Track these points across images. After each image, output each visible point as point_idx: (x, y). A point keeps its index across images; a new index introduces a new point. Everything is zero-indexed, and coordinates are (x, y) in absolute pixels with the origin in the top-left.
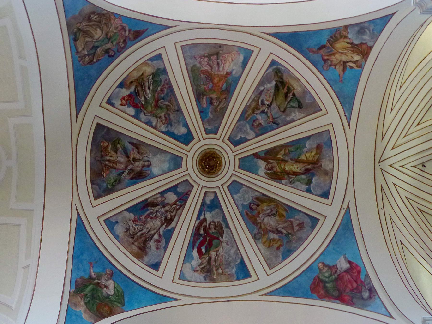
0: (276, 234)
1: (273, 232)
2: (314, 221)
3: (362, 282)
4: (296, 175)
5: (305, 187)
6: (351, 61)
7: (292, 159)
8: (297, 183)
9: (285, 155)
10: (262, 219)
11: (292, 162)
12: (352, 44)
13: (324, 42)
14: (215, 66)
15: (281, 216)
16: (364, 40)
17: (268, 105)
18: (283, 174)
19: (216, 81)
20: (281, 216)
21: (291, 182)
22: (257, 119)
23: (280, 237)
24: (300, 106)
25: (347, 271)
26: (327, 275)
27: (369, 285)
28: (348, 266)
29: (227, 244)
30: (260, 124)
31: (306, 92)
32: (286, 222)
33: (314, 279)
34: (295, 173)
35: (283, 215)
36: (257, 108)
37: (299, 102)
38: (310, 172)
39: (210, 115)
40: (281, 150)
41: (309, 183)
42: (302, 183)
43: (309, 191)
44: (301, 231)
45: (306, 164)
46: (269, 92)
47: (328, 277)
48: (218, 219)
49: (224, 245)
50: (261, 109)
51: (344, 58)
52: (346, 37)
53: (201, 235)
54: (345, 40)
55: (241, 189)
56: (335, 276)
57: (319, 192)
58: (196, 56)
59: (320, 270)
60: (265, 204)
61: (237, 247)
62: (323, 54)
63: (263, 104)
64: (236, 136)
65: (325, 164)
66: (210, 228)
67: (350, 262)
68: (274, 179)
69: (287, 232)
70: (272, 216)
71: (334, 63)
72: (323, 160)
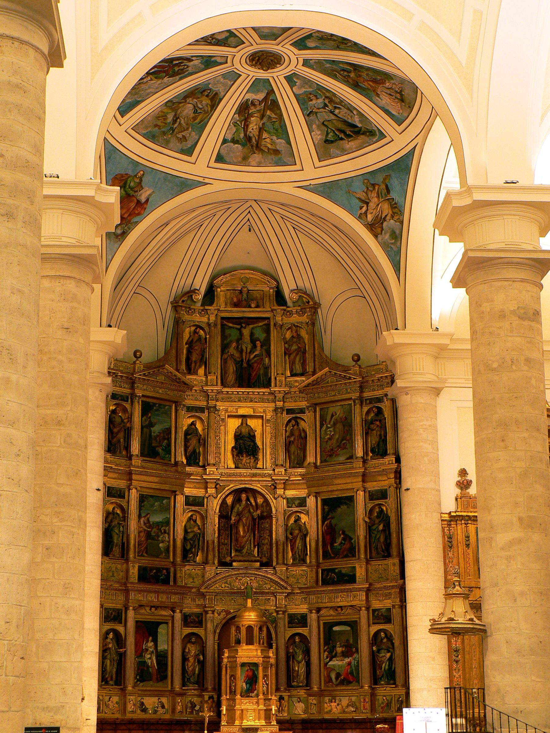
0: (173, 118)
1: (175, 115)
2: (189, 152)
3: (130, 221)
4: (244, 128)
5: (229, 137)
6: (367, 210)
7: (263, 124)
8: (234, 129)
9: (270, 118)
10: (191, 102)
11: (261, 124)
12: (385, 219)
13: (393, 195)
14: (389, 92)
15: (195, 119)
16: (385, 233)
17: (334, 111)
18: (246, 115)
19: (371, 83)
20: (195, 119)
21: (236, 123)
22: (317, 98)
23: (169, 123)
24: (327, 141)
25: (138, 202)
26: (132, 184)
27: (128, 229)
28: (143, 199)
29: (161, 83)
30: (311, 100)
31: (344, 152)
32: (187, 124)
33: (126, 174)
34: (246, 127)
35: (195, 120)
36: (331, 101)
37: (332, 142)
38: (248, 143)
39: (328, 65)
40: (275, 114)
41: (234, 141)
42: (234, 134)
43: (225, 141)
44: (177, 141)
45: (257, 138)
46: (350, 117)
47: (130, 187)
48: (190, 70)
49: (159, 82)
50: (329, 105)
51: (372, 205)
52: (392, 217)
53: (172, 62)
54: (389, 215)
55: (229, 80)
56: (132, 193)
57: (223, 152)
58: (403, 85)
59: (136, 176)
60: (210, 103)
61: (157, 93)
62: (381, 187)
63: (335, 108)
64: (298, 79)
65: (256, 157)
66: (179, 66)
67: (147, 200)
68: (241, 108)
69: (176, 128)
70: (194, 111)
71: (369, 193)
72: (261, 156)
